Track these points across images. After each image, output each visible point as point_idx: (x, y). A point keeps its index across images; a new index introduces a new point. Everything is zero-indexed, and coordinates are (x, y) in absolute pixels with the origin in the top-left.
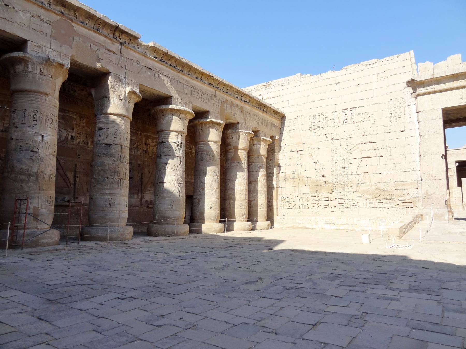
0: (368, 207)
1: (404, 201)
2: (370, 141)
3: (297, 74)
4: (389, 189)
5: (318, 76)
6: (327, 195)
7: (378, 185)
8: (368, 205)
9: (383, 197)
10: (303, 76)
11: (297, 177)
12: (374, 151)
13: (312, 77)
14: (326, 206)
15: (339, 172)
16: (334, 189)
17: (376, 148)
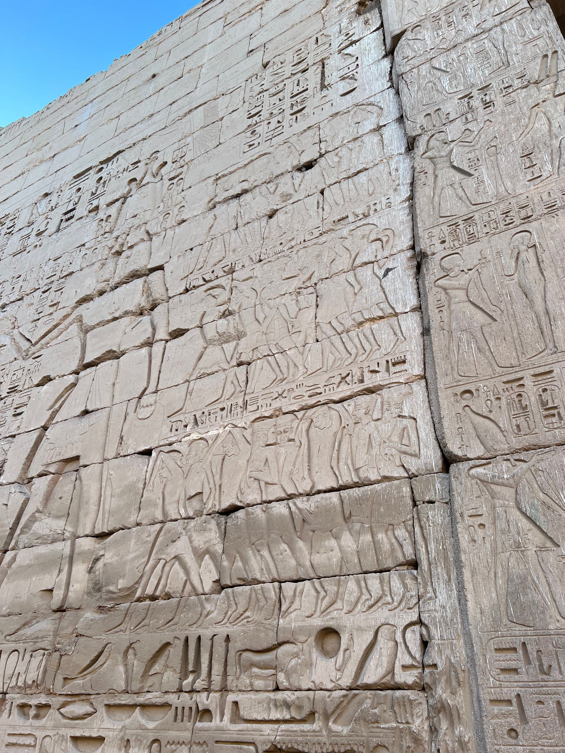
4: (175, 579)
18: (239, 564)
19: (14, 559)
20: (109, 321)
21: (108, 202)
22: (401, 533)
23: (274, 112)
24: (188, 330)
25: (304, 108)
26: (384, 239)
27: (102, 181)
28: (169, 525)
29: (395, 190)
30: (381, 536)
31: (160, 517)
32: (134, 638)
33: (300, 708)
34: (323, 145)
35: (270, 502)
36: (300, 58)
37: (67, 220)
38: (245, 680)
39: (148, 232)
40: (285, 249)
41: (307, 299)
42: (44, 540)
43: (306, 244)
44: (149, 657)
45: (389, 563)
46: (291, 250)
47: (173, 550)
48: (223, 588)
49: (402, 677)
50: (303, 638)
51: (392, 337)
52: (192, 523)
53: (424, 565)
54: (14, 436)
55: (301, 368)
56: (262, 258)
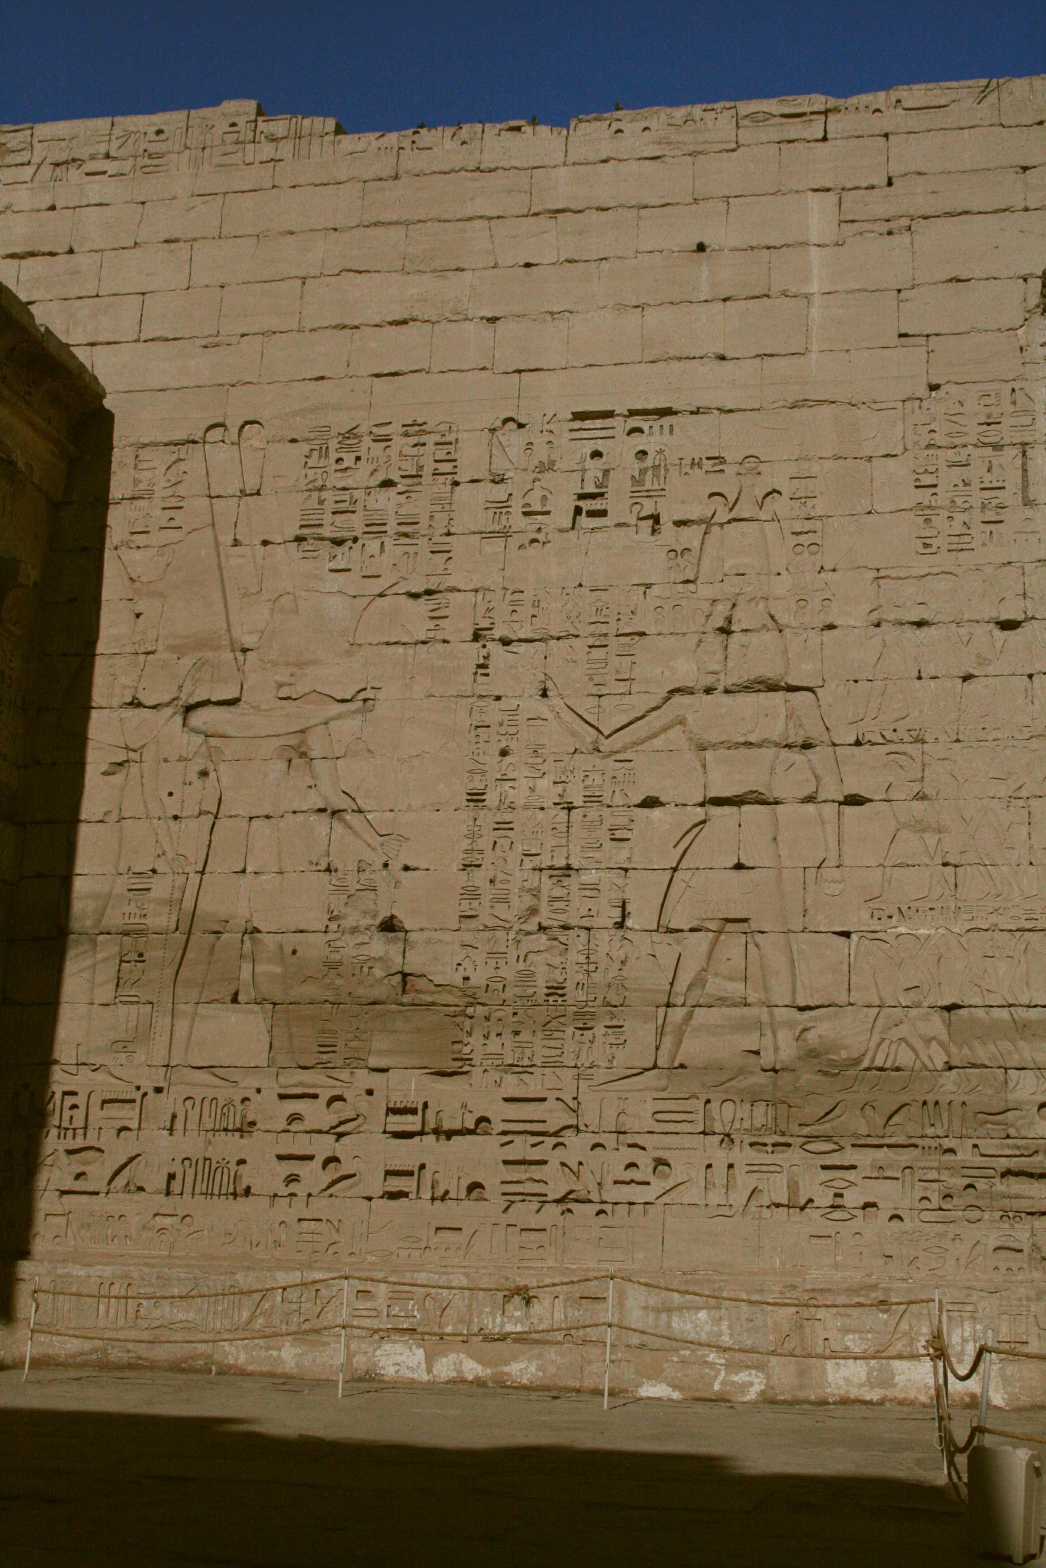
0: (738, 1198)
1: (1013, 1163)
2: (771, 671)
3: (230, 106)
4: (905, 1057)
5: (392, 138)
6: (409, 1086)
7: (823, 1029)
8: (745, 1182)
10: (279, 126)
11: (161, 919)
12: (796, 756)
13: (347, 142)
14: (396, 1184)
15: (520, 903)
16: (475, 1041)
17: (814, 731)
18: (965, 1051)
19: (689, 1016)
20: (737, 745)
21: (676, 518)
23: (959, 501)
24: (870, 801)
25: (1001, 522)
27: (649, 462)
28: (886, 1011)
31: (878, 1003)
33: (1027, 1148)
35: (992, 1007)
36: (989, 416)
37: (591, 514)
38: (981, 1131)
40: (990, 738)
42: (722, 1001)
43: (1016, 743)
44: (888, 1113)
46: (995, 743)
48: (951, 1068)
50: (1028, 1107)
52: (913, 1012)
54: (626, 870)
55: (1016, 889)
56: (961, 737)
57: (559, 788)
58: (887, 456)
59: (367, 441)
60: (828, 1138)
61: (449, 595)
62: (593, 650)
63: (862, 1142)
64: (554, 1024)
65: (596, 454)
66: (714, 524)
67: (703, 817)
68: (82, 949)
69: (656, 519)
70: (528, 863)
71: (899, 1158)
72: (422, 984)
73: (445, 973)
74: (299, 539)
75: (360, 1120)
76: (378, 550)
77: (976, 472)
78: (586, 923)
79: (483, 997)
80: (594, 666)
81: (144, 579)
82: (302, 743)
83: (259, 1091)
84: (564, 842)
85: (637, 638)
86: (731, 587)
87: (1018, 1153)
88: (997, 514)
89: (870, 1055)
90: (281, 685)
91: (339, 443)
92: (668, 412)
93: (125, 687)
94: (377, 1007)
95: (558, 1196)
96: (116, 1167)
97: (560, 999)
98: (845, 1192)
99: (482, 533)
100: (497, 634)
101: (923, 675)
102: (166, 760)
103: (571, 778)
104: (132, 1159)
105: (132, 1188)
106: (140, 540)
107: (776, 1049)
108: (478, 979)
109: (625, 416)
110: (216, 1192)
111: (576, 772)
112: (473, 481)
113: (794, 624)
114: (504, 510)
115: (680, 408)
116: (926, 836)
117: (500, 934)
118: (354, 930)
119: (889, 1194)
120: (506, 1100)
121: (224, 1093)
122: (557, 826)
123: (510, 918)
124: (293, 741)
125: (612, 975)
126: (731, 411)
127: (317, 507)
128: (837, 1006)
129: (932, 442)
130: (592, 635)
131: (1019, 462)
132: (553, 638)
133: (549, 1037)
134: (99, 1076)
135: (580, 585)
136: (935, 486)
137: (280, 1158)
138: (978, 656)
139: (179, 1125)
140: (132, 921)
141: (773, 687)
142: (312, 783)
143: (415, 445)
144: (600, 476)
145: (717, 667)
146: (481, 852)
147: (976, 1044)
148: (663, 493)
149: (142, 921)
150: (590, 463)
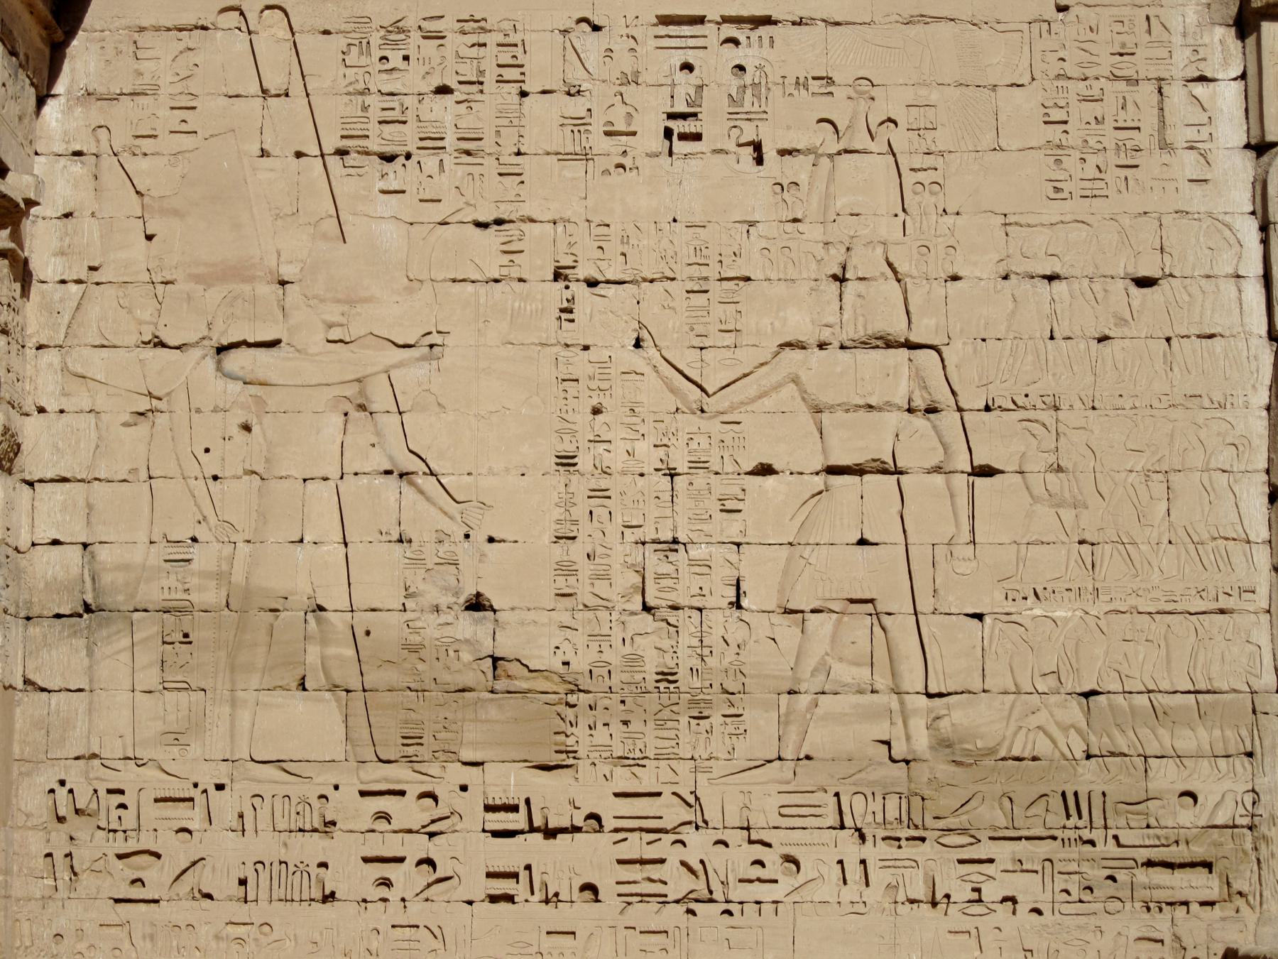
4: (1043, 746)
6: (510, 781)
7: (958, 716)
9: (991, 814)
12: (919, 422)
16: (581, 731)
18: (1105, 739)
22: (1244, 733)
23: (1092, 142)
24: (1003, 472)
25: (1136, 166)
26: (1241, 448)
27: (748, 79)
29: (1254, 386)
30: (1228, 733)
31: (1014, 689)
32: (1007, 789)
34: (1167, 258)
36: (1123, 45)
37: (683, 137)
39: (890, 265)
41: (1159, 489)
43: (1154, 412)
45: (1232, 751)
47: (1034, 721)
48: (1089, 757)
49: (1239, 821)
51: (1245, 564)
52: (1053, 699)
53: (1259, 756)
54: (738, 545)
55: (1156, 569)
56: (1096, 405)
57: (662, 451)
58: (1012, 85)
59: (416, 36)
60: (963, 831)
61: (526, 227)
62: (691, 295)
63: (1000, 834)
64: (666, 714)
65: (687, 67)
66: (821, 155)
67: (822, 487)
68: (114, 628)
69: (757, 147)
70: (630, 536)
71: (1038, 850)
72: (514, 668)
73: (541, 657)
74: (342, 153)
75: (455, 818)
76: (437, 169)
77: (1108, 108)
78: (697, 602)
79: (585, 683)
80: (694, 314)
81: (154, 193)
82: (362, 393)
83: (336, 787)
84: (668, 512)
85: (741, 283)
86: (846, 227)
87: (1158, 843)
88: (1132, 157)
89: (1007, 743)
90: (331, 326)
91: (383, 38)
92: (767, 21)
93: (141, 323)
94: (466, 694)
95: (680, 897)
96: (178, 872)
97: (671, 686)
98: (984, 887)
99: (557, 154)
100: (583, 272)
101: (1056, 335)
102: (198, 411)
103: (673, 440)
104: (194, 863)
105: (197, 895)
106: (147, 145)
107: (908, 738)
108: (580, 664)
109: (718, 23)
110: (297, 898)
111: (680, 434)
112: (544, 92)
113: (915, 273)
114: (582, 128)
115: (780, 18)
116: (1062, 511)
117: (603, 614)
118: (437, 609)
119: (1028, 888)
120: (616, 795)
121: (296, 789)
122: (660, 495)
123: (614, 598)
124: (351, 391)
125: (728, 660)
126: (837, 24)
127: (360, 113)
128: (970, 692)
129: (1062, 72)
130: (691, 279)
131: (1156, 97)
132: (645, 280)
133: (660, 727)
134: (150, 773)
135: (675, 220)
136: (1066, 122)
137: (366, 860)
138: (1115, 315)
139: (249, 826)
140: (173, 596)
141: (889, 345)
142: (374, 440)
143: (473, 45)
144: (692, 92)
145: (833, 319)
146: (575, 522)
147: (1116, 733)
148: (765, 116)
149: (185, 596)
150: (682, 77)
